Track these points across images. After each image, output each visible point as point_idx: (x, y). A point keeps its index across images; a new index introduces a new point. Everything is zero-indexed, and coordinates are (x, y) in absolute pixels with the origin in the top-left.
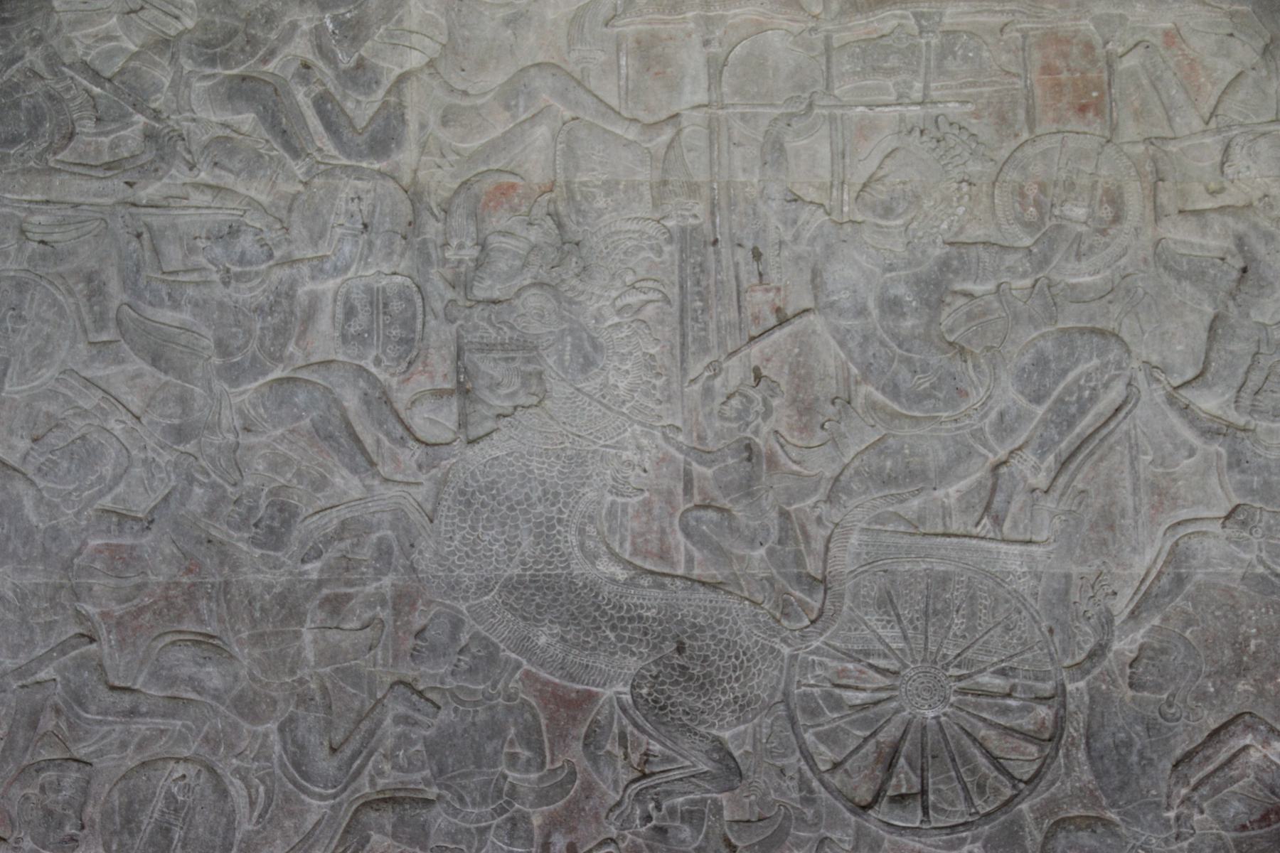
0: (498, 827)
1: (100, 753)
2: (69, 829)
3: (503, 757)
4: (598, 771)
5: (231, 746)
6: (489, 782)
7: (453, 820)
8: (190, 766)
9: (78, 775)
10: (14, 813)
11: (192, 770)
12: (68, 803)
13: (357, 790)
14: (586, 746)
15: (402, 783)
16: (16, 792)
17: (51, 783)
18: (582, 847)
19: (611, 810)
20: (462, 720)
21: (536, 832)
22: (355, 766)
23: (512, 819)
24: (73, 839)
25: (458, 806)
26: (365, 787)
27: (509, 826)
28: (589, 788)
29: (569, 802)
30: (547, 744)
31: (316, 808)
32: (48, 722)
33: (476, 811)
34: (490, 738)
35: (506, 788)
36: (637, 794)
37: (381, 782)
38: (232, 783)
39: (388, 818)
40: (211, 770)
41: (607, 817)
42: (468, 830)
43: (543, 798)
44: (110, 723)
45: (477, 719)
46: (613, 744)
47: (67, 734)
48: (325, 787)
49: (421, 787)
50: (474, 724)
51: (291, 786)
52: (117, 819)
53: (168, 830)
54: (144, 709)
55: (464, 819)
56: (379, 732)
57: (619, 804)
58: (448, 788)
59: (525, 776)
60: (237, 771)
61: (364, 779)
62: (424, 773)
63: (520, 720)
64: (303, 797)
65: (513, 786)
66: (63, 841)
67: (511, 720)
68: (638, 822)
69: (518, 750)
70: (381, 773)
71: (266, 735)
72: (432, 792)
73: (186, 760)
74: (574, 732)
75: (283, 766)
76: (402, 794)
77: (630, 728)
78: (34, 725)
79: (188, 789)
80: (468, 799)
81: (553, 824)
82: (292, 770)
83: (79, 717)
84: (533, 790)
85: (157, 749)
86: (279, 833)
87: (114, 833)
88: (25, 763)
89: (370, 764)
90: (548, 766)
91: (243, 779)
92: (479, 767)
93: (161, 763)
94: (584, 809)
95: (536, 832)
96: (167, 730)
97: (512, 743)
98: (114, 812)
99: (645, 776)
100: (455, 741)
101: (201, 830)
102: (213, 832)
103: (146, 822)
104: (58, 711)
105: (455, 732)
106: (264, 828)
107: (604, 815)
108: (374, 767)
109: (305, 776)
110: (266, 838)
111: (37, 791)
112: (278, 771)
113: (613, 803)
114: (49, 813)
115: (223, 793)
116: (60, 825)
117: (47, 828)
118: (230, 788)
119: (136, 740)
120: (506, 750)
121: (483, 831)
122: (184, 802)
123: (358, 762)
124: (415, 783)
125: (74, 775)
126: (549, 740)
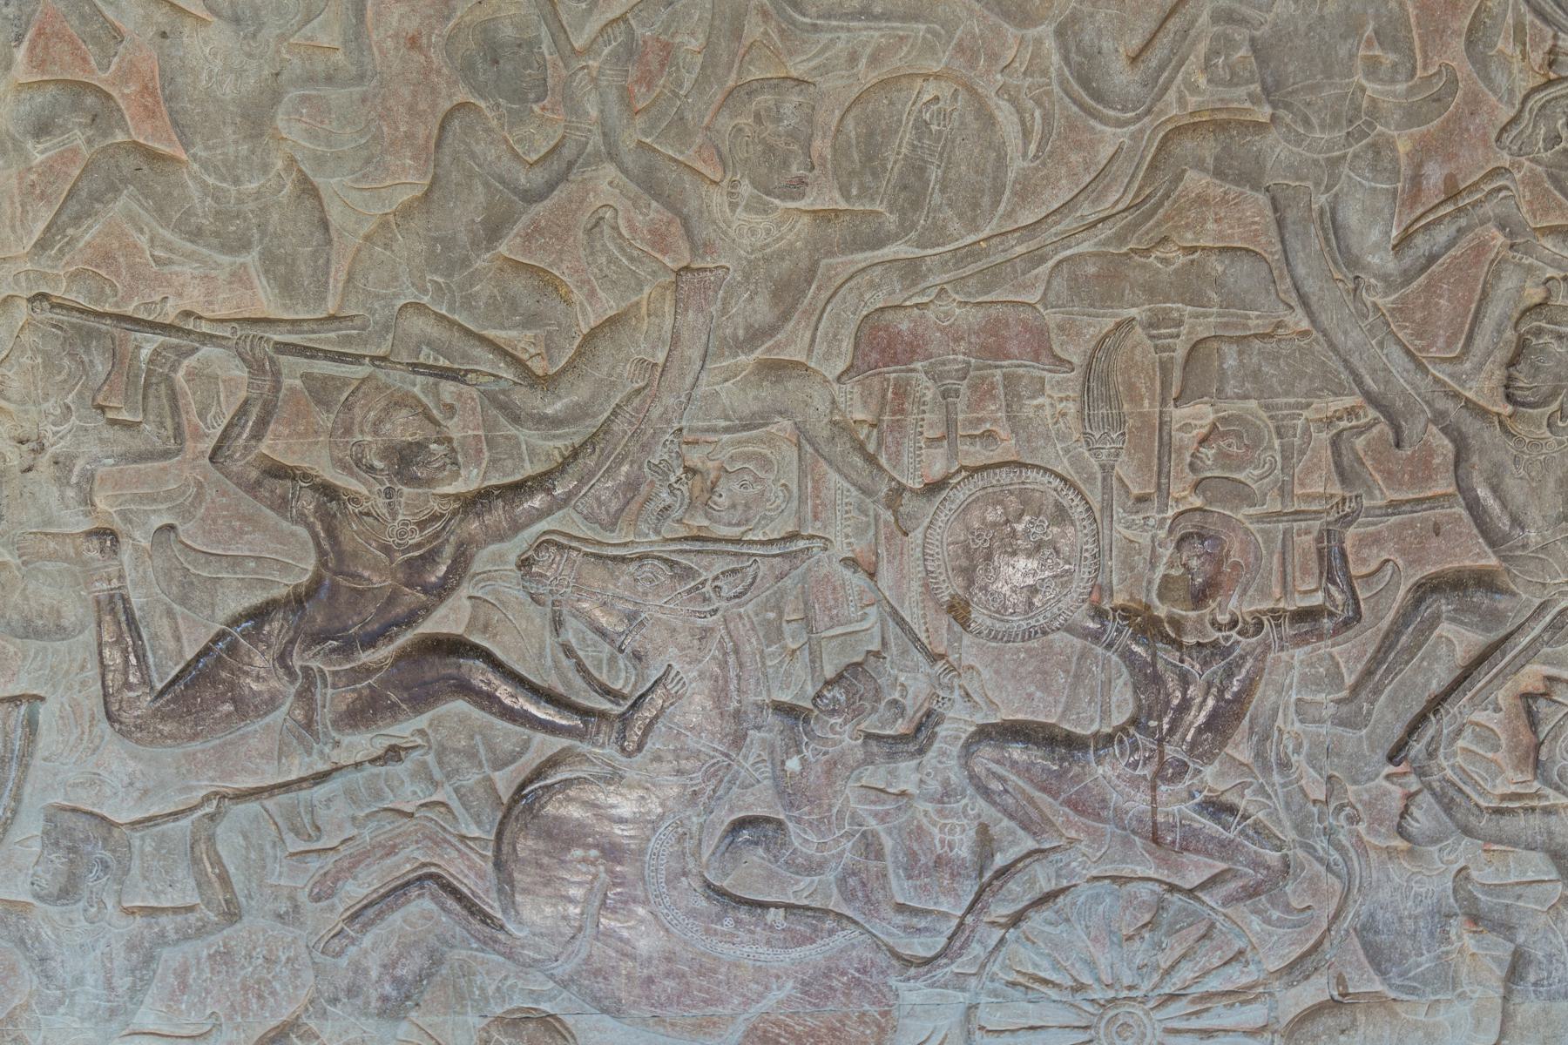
0: (1356, 156)
1: (824, 69)
2: (795, 170)
3: (1359, 62)
4: (1488, 80)
5: (993, 57)
6: (1343, 97)
7: (1295, 149)
8: (943, 84)
9: (801, 99)
10: (725, 150)
11: (946, 89)
12: (793, 135)
13: (1162, 112)
14: (1470, 43)
15: (1222, 100)
16: (725, 123)
17: (768, 109)
18: (1464, 180)
19: (1504, 129)
20: (1305, 13)
21: (1403, 161)
22: (1161, 81)
23: (1373, 145)
24: (802, 181)
25: (1302, 131)
26: (1171, 109)
27: (1370, 155)
28: (1474, 101)
29: (1448, 121)
30: (1417, 43)
31: (1110, 138)
32: (754, 29)
33: (1326, 136)
34: (1344, 37)
35: (1365, 105)
36: (1543, 107)
37: (1193, 101)
38: (998, 107)
39: (1208, 148)
40: (971, 90)
41: (1498, 139)
42: (1316, 162)
43: (1412, 116)
44: (835, 29)
45: (1326, 11)
46: (1506, 39)
47: (779, 44)
48: (1124, 109)
49: (1247, 105)
50: (1322, 18)
51: (1075, 109)
52: (856, 156)
53: (923, 169)
54: (878, 10)
55: (1309, 148)
56: (1193, 33)
57: (1514, 121)
58: (1288, 106)
59: (1388, 88)
60: (1002, 90)
61: (1172, 95)
62: (1252, 87)
63: (1383, 10)
64: (1092, 122)
65: (1373, 100)
66: (790, 185)
67: (1371, 11)
68: (1541, 144)
69: (1378, 52)
70: (1194, 89)
71: (1039, 41)
72: (1264, 113)
73: (937, 76)
74: (1455, 25)
75: (1063, 83)
76: (1224, 116)
77: (1529, 17)
78: (737, 34)
79: (943, 115)
80: (1315, 121)
81: (1423, 151)
82: (1076, 87)
83: (793, 23)
84: (1400, 106)
85: (896, 63)
86: (1064, 171)
87: (852, 174)
88: (731, 83)
89: (1180, 76)
90: (1419, 74)
91: (1013, 101)
92: (1330, 77)
93: (904, 81)
94: (1467, 130)
95: (1403, 161)
96: (908, 37)
97: (1369, 44)
98: (850, 146)
99: (1550, 83)
100: (1297, 42)
101: (963, 168)
102: (981, 172)
103: (892, 159)
104: (765, 14)
105: (1296, 29)
106: (1044, 164)
107: (1494, 136)
108: (1185, 81)
109: (1098, 96)
110: (1046, 177)
111: (750, 121)
112: (1056, 88)
113: (1505, 120)
114: (770, 149)
115: (989, 121)
116: (785, 164)
117: (770, 168)
118: (997, 112)
119: (869, 50)
120: (1361, 53)
121: (1334, 163)
122: (940, 132)
123: (1166, 74)
124: (1239, 100)
125: (796, 99)
126: (1420, 36)
